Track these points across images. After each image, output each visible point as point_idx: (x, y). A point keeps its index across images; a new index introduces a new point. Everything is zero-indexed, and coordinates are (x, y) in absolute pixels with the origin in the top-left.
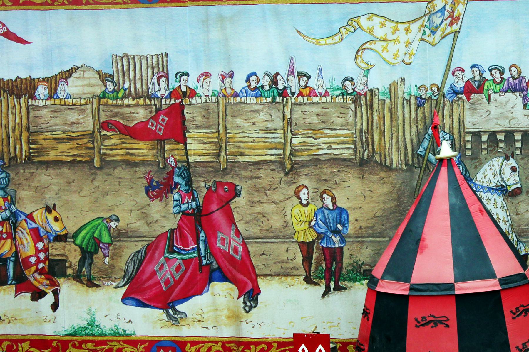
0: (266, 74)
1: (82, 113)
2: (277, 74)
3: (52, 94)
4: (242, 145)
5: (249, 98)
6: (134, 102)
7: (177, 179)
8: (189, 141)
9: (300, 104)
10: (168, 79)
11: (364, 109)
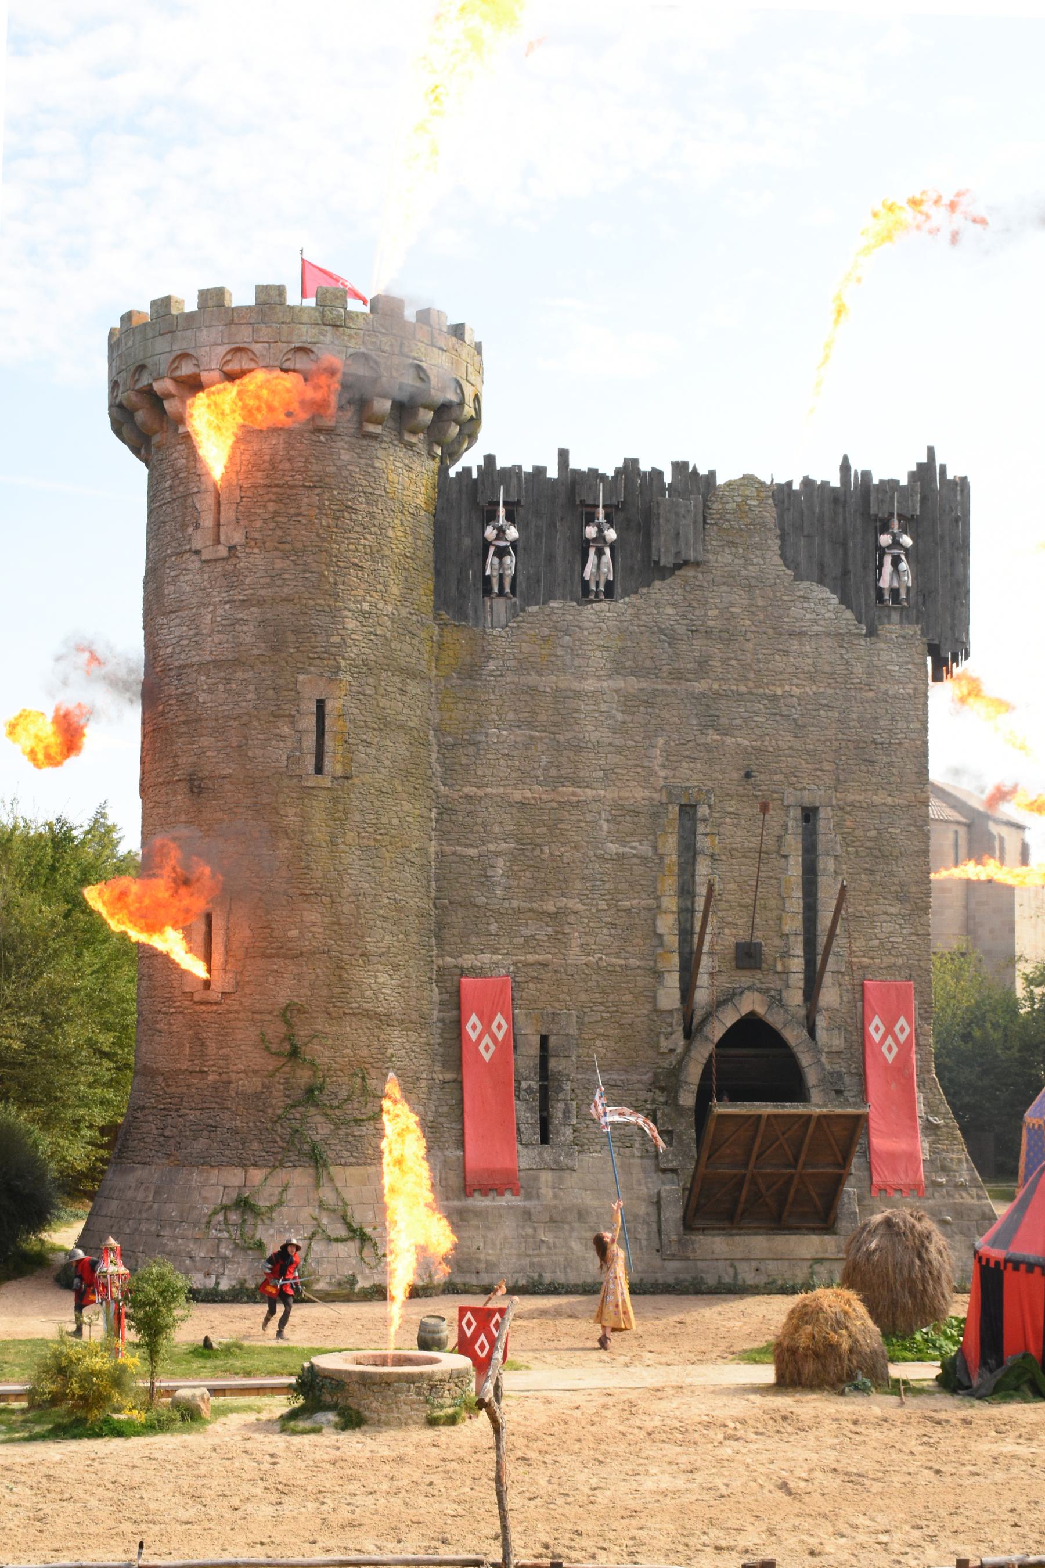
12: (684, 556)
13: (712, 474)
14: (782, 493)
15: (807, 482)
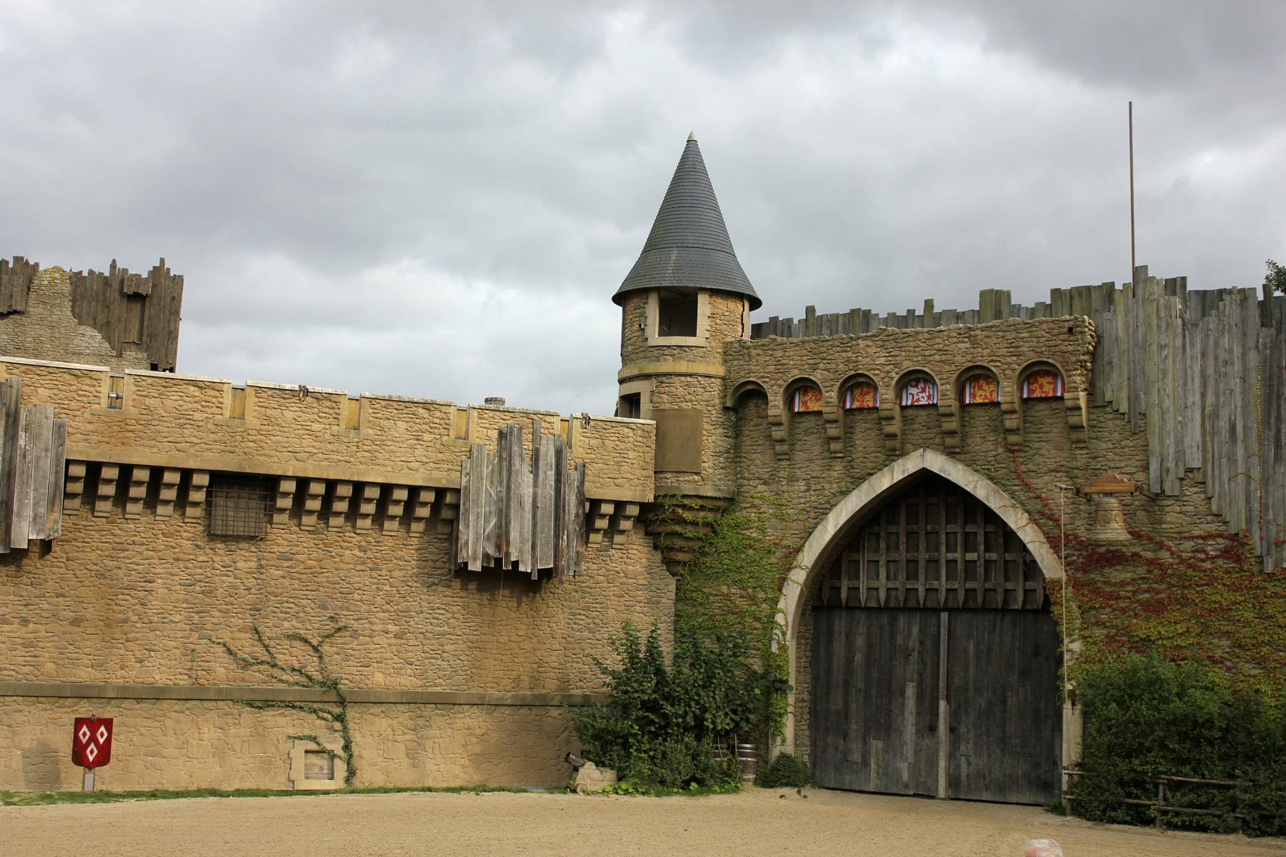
12: (14, 308)
13: (37, 265)
14: (76, 278)
15: (91, 272)
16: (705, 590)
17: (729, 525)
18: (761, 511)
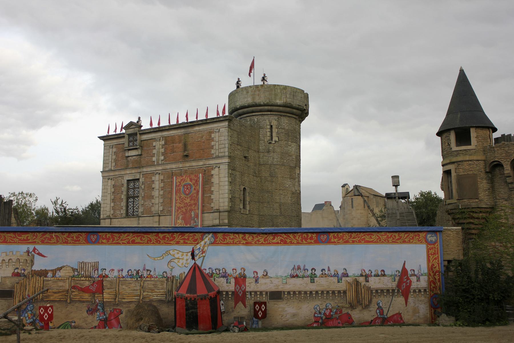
0: (135, 270)
1: (65, 283)
2: (139, 270)
3: (54, 275)
4: (124, 295)
5: (128, 279)
6: (85, 279)
7: (99, 307)
8: (104, 293)
9: (147, 281)
10: (98, 271)
11: (170, 283)
16: (485, 244)
17: (493, 218)
18: (506, 211)
